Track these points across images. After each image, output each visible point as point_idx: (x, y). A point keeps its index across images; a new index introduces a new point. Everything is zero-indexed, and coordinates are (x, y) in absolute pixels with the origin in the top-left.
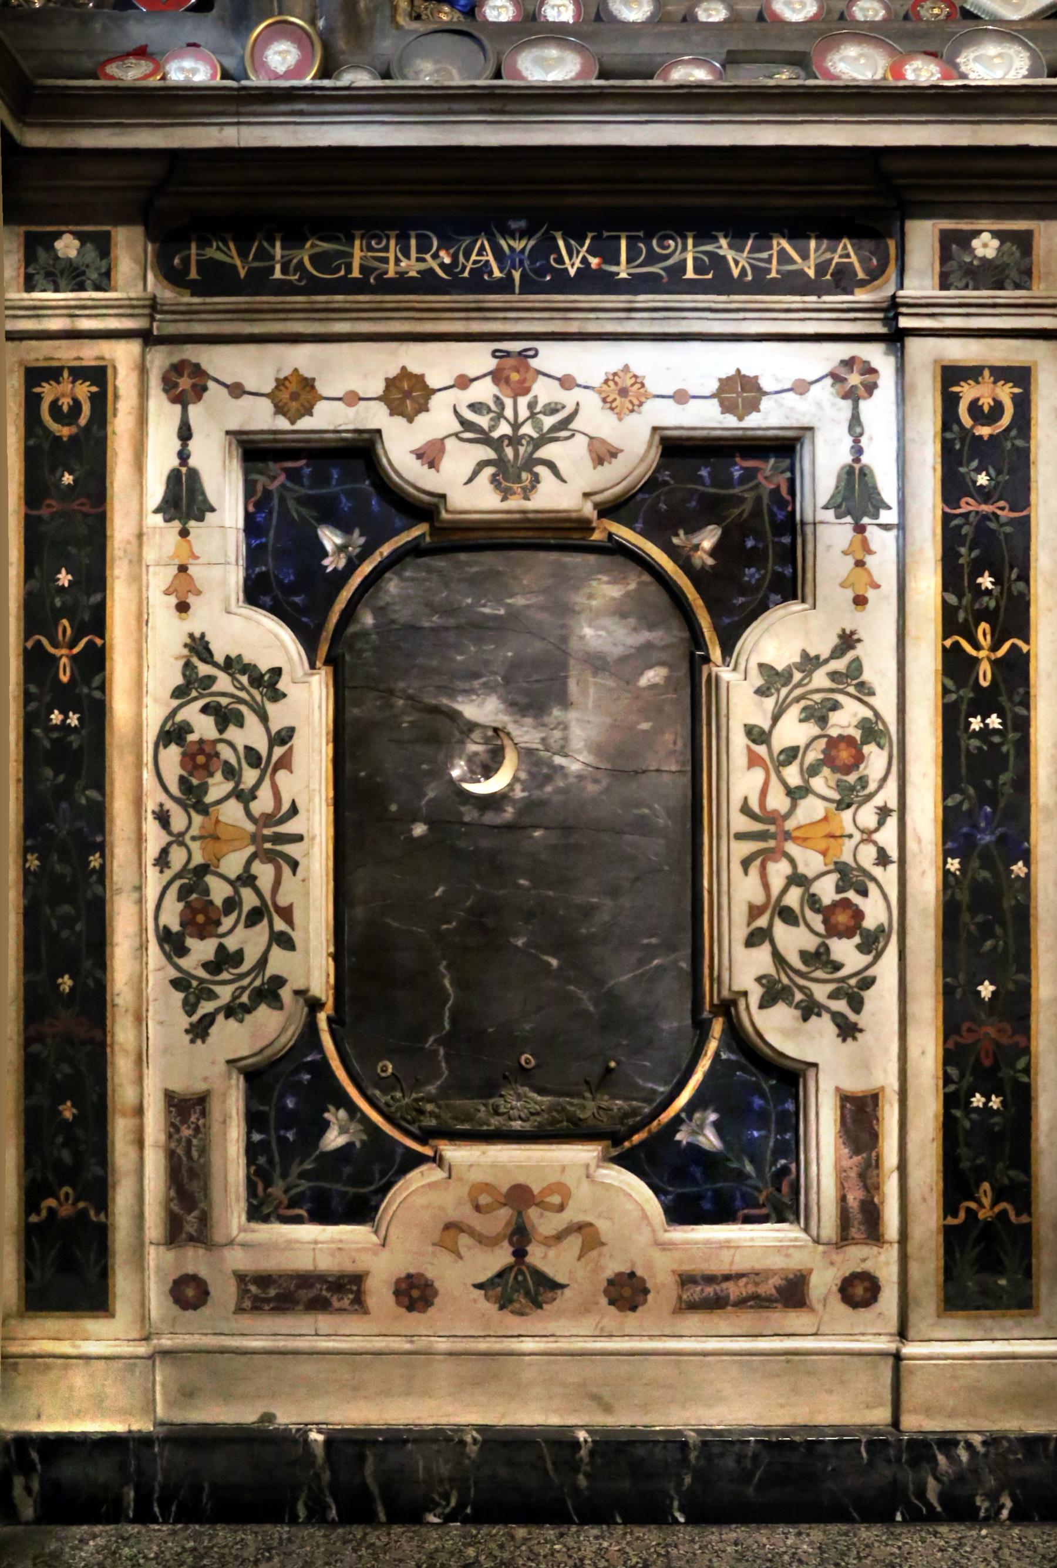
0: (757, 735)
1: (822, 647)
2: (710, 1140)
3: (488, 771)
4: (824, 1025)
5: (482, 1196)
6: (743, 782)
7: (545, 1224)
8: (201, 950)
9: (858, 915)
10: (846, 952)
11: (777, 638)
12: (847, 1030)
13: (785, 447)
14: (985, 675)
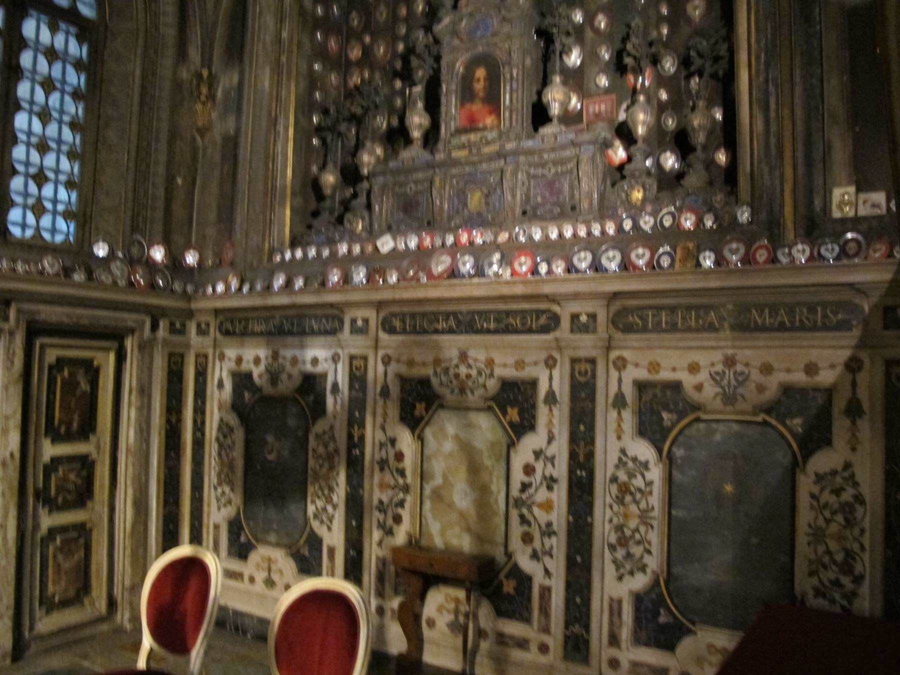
0: (314, 450)
1: (327, 428)
2: (307, 553)
3: (270, 452)
4: (325, 528)
5: (263, 558)
6: (311, 463)
7: (273, 567)
8: (219, 490)
9: (332, 499)
10: (330, 508)
11: (320, 426)
12: (329, 529)
13: (324, 376)
14: (356, 439)
